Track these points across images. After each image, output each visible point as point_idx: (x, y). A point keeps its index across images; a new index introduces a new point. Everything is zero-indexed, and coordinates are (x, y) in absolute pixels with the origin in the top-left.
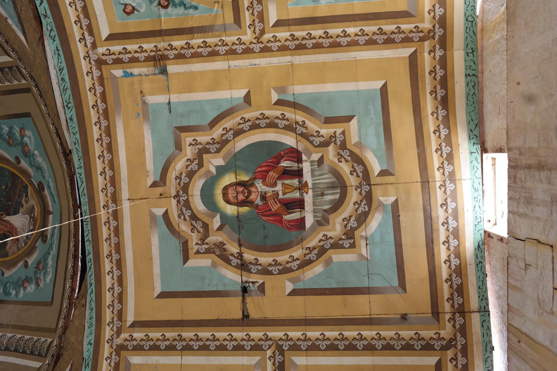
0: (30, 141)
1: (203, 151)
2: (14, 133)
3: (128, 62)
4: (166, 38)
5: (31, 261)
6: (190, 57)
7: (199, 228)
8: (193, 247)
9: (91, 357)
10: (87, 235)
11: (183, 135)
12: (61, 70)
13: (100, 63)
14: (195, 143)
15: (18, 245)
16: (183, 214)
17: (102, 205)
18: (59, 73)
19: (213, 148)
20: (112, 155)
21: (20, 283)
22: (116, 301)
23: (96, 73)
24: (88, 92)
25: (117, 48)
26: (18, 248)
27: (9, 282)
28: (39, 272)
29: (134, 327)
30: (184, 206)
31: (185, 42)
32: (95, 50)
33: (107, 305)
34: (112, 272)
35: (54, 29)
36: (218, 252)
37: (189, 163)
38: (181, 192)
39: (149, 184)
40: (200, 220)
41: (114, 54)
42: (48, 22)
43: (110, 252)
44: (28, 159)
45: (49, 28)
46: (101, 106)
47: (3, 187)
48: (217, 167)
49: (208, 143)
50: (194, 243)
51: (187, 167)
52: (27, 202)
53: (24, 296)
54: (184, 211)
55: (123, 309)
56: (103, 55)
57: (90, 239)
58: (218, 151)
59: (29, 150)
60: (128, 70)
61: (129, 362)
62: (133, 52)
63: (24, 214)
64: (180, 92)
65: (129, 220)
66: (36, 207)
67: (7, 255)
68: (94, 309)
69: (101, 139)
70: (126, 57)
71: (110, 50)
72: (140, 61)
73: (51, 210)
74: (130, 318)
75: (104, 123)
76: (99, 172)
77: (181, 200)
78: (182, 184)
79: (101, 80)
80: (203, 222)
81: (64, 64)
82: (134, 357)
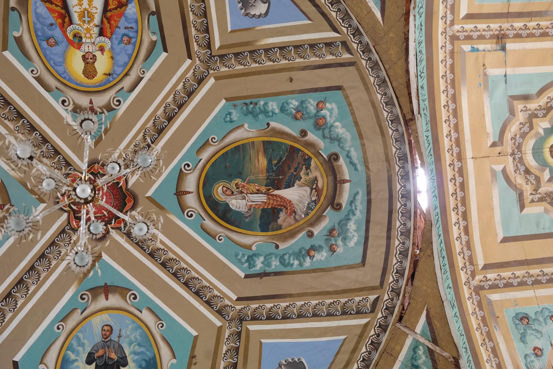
0: (331, 113)
1: (533, 116)
2: (307, 107)
4: (510, 20)
5: (316, 231)
6: (526, 37)
7: (532, 181)
8: (528, 197)
9: (454, 298)
10: (434, 191)
11: (515, 102)
12: (420, 43)
13: (454, 38)
14: (526, 110)
15: (295, 217)
17: (448, 164)
18: (418, 46)
19: (540, 114)
21: (304, 252)
23: (449, 47)
24: (440, 63)
25: (469, 26)
27: (288, 253)
28: (333, 239)
29: (486, 269)
31: (523, 24)
32: (452, 27)
35: (424, 7)
37: (521, 126)
39: (489, 144)
40: (533, 174)
41: (466, 31)
43: (457, 205)
44: (320, 132)
45: (420, 5)
46: (449, 76)
47: (275, 162)
48: (545, 129)
49: (536, 109)
50: (529, 194)
52: (308, 174)
53: (311, 265)
54: (519, 167)
56: (458, 31)
57: (437, 195)
58: (545, 116)
59: (325, 123)
60: (475, 46)
61: (490, 300)
62: (481, 31)
63: (301, 186)
64: (514, 67)
65: (473, 176)
67: (280, 228)
68: (446, 257)
69: (448, 105)
70: (475, 35)
71: (463, 28)
72: (486, 39)
73: (347, 177)
74: (481, 263)
75: (451, 91)
76: (445, 135)
77: (516, 157)
78: (517, 144)
79: (452, 53)
81: (423, 38)
82: (493, 295)
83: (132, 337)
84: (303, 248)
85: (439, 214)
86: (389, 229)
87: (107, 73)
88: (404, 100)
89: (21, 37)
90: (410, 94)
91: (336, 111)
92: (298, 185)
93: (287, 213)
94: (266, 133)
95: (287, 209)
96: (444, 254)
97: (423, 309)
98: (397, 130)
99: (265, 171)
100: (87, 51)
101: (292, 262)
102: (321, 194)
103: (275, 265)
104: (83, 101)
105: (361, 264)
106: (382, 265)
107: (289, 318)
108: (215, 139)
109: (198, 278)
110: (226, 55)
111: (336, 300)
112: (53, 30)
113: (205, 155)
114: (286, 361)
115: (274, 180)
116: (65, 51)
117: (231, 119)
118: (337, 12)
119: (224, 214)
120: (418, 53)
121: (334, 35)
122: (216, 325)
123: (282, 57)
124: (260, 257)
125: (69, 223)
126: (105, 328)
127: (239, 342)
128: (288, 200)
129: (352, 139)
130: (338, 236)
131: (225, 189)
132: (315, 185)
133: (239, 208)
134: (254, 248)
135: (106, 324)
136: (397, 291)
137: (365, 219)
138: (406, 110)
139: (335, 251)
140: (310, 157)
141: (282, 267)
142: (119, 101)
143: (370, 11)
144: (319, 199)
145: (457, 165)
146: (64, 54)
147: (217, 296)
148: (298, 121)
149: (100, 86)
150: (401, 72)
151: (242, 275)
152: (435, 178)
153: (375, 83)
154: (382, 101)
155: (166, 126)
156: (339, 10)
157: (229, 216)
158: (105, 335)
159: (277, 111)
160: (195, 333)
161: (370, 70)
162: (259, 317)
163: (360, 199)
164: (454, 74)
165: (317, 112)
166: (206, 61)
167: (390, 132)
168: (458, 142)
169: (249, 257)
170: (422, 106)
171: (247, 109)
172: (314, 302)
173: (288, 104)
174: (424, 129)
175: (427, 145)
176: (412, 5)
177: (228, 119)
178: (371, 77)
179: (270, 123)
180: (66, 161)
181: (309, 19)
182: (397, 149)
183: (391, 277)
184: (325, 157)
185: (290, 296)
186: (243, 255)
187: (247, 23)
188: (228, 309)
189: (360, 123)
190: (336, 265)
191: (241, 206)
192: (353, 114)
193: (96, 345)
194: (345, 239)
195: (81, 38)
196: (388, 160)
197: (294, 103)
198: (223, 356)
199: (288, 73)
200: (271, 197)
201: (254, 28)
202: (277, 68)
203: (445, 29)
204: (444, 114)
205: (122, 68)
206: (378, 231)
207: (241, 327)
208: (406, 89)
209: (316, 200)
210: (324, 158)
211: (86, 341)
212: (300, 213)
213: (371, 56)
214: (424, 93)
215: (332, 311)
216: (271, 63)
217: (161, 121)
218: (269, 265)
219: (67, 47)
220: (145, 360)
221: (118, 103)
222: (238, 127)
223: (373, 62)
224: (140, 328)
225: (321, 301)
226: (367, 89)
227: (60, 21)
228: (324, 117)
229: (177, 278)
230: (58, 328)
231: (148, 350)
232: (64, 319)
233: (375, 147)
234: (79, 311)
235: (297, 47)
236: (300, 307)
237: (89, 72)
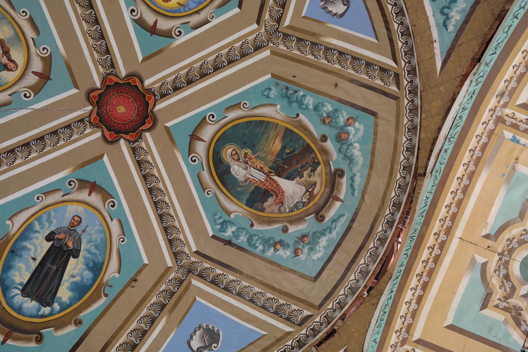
2: (338, 117)
3: (522, 131)
5: (292, 229)
7: (507, 288)
8: (495, 300)
10: (408, 250)
12: (464, 109)
13: (500, 120)
15: (280, 208)
16: (499, 270)
17: (434, 232)
20: (464, 196)
21: (271, 242)
22: (409, 315)
23: (491, 126)
24: (475, 137)
26: (279, 210)
28: (302, 243)
30: (503, 264)
32: (503, 109)
33: (400, 315)
34: (415, 290)
35: (485, 77)
36: (514, 313)
37: (524, 233)
38: (506, 253)
39: (483, 234)
40: (511, 282)
41: (516, 119)
42: (483, 70)
43: (422, 273)
44: (339, 145)
45: (481, 74)
46: (478, 153)
47: (288, 151)
51: (521, 235)
52: (310, 176)
53: (272, 256)
54: (501, 269)
55: (413, 324)
56: (507, 115)
57: (409, 254)
59: (347, 139)
60: (518, 137)
63: (299, 184)
65: (452, 255)
66: (318, 186)
67: (263, 210)
68: (386, 315)
69: (462, 179)
71: (514, 115)
73: (342, 197)
74: (417, 335)
75: (472, 168)
76: (445, 204)
77: (503, 259)
78: (510, 247)
80: (513, 285)
81: (469, 106)
83: (94, 238)
84: (273, 238)
85: (402, 273)
86: (353, 262)
87: (181, 3)
88: (424, 154)
90: (431, 151)
91: (361, 133)
92: (297, 182)
93: (275, 200)
94: (292, 121)
95: (277, 197)
96: (388, 310)
97: (343, 347)
98: (404, 178)
99: (275, 155)
101: (257, 245)
102: (313, 200)
103: (242, 240)
104: (150, 18)
105: (313, 279)
106: (330, 290)
107: (229, 291)
108: (246, 105)
109: (173, 217)
110: (290, 36)
111: (275, 298)
113: (232, 115)
114: (206, 326)
115: (280, 166)
117: (268, 94)
118: (404, 44)
119: (222, 173)
120: (458, 118)
121: (392, 63)
122: (166, 264)
123: (337, 61)
124: (233, 227)
125: (90, 116)
126: (76, 218)
127: (178, 289)
128: (282, 190)
129: (363, 165)
130: (307, 244)
131: (234, 152)
132: (312, 189)
133: (238, 175)
134: (232, 216)
135: (78, 215)
136: (330, 319)
137: (338, 242)
138: (421, 163)
139: (298, 256)
140: (319, 162)
141: (247, 245)
142: (180, 32)
143: (433, 57)
144: (309, 202)
145: (442, 237)
147: (181, 240)
148: (324, 126)
149: (169, 11)
150: (434, 127)
151: (211, 234)
152: (415, 238)
153: (407, 126)
154: (405, 145)
155: (210, 73)
156: (406, 43)
157: (225, 177)
158: (73, 224)
159: (311, 107)
160: (146, 261)
161: (408, 111)
162: (205, 277)
163: (343, 222)
164: (483, 153)
165: (345, 125)
166: (270, 33)
167: (398, 176)
168: (454, 218)
169: (224, 221)
170: (437, 167)
171: (286, 92)
172: (257, 290)
173: (323, 105)
174: (428, 190)
175: (423, 205)
176: (474, 71)
177: (266, 93)
178: (405, 118)
179: (300, 114)
180: (112, 62)
181: (377, 39)
182: (396, 195)
183: (331, 304)
184: (333, 169)
185: (241, 273)
186: (221, 217)
187: (321, 15)
188: (184, 256)
189: (376, 154)
190: (293, 268)
191: (240, 174)
192: (374, 143)
193: (61, 228)
194: (311, 249)
196: (383, 200)
197: (329, 108)
198: (158, 293)
199: (336, 78)
200: (269, 179)
201: (325, 23)
202: (329, 68)
203: (495, 107)
204: (453, 185)
205: (195, 5)
206: (343, 258)
207: (186, 276)
208: (430, 145)
209: (305, 202)
210: (331, 169)
211: (54, 221)
212: (286, 207)
213: (415, 99)
214: (445, 157)
215: (268, 305)
216: (326, 62)
217: (208, 67)
218: (237, 237)
220: (94, 262)
221: (178, 34)
222: (271, 105)
223: (414, 105)
224: (104, 233)
225: (263, 292)
226: (397, 128)
228: (348, 133)
229: (156, 207)
230: (38, 199)
231: (100, 255)
233: (378, 183)
234: (62, 193)
235: (355, 58)
236: (244, 287)
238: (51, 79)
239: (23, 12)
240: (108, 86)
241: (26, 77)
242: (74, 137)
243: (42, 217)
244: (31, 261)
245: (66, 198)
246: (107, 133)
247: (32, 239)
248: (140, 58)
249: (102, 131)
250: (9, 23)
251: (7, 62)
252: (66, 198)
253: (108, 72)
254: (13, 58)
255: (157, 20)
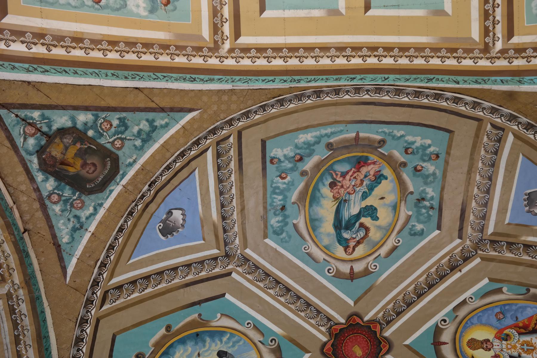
89: (503, 293)
100: (494, 344)
104: (446, 337)
112: (512, 319)
116: (492, 326)
125: (336, 324)
146: (488, 325)
149: (461, 351)
180: (391, 321)
195: (506, 340)
211: (236, 348)
219: (496, 328)
227: (521, 325)
230: (248, 324)
232: (256, 328)
234: (261, 339)
237: (474, 344)
238: (352, 281)
239: (399, 241)
240: (369, 327)
241: (345, 264)
242: (312, 321)
243: (234, 337)
244: (196, 354)
245: (260, 345)
246: (329, 346)
247: (214, 342)
248: (407, 342)
249: (329, 341)
250: (385, 235)
251: (352, 247)
252: (260, 345)
253: (382, 322)
254: (356, 249)
255: (448, 343)
